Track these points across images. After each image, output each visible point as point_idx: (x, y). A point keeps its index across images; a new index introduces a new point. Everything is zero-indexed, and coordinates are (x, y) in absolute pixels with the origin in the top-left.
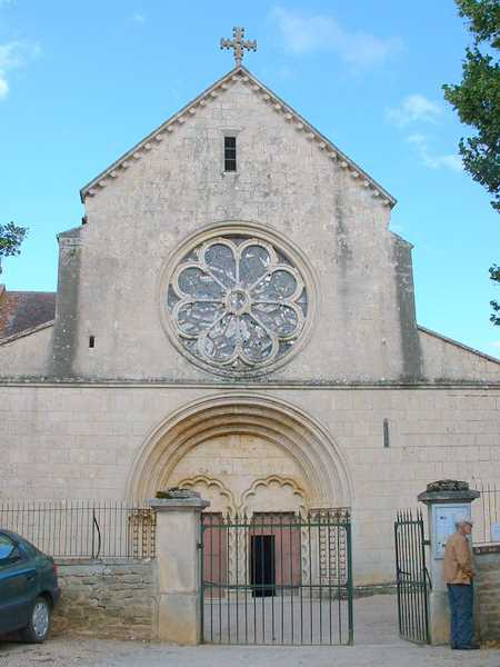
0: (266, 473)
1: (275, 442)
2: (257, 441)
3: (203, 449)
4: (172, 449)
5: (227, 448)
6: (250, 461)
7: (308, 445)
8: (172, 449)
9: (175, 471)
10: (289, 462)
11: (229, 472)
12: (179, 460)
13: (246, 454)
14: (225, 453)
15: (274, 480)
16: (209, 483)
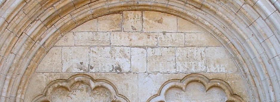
0: (182, 69)
1: (194, 21)
2: (171, 21)
3: (82, 34)
4: (32, 30)
5: (123, 34)
6: (158, 51)
7: (251, 24)
8: (32, 30)
9: (41, 68)
10: (218, 53)
11: (126, 69)
12: (45, 50)
13: (152, 41)
14: (118, 39)
15: (194, 79)
16: (93, 85)
